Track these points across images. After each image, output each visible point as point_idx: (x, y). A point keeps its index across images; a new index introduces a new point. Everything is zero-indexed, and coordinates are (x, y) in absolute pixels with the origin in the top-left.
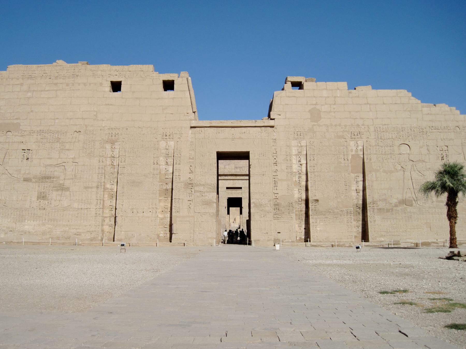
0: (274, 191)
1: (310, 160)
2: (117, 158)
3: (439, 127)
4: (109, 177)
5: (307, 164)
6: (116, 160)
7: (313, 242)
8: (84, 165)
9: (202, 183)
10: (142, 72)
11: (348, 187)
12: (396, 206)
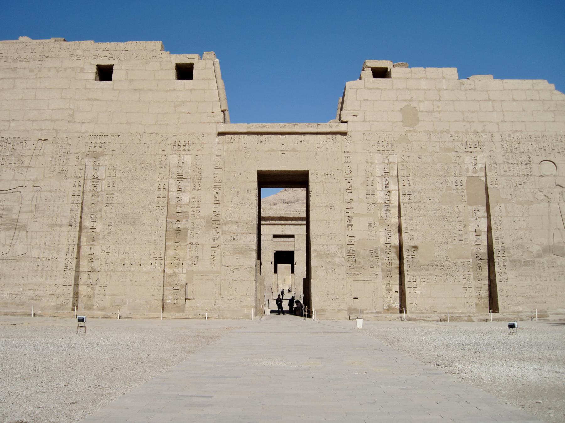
1: (404, 185)
4: (89, 209)
5: (399, 190)
6: (100, 184)
7: (411, 313)
8: (50, 191)
9: (234, 220)
10: (145, 52)
11: (463, 226)
12: (539, 256)
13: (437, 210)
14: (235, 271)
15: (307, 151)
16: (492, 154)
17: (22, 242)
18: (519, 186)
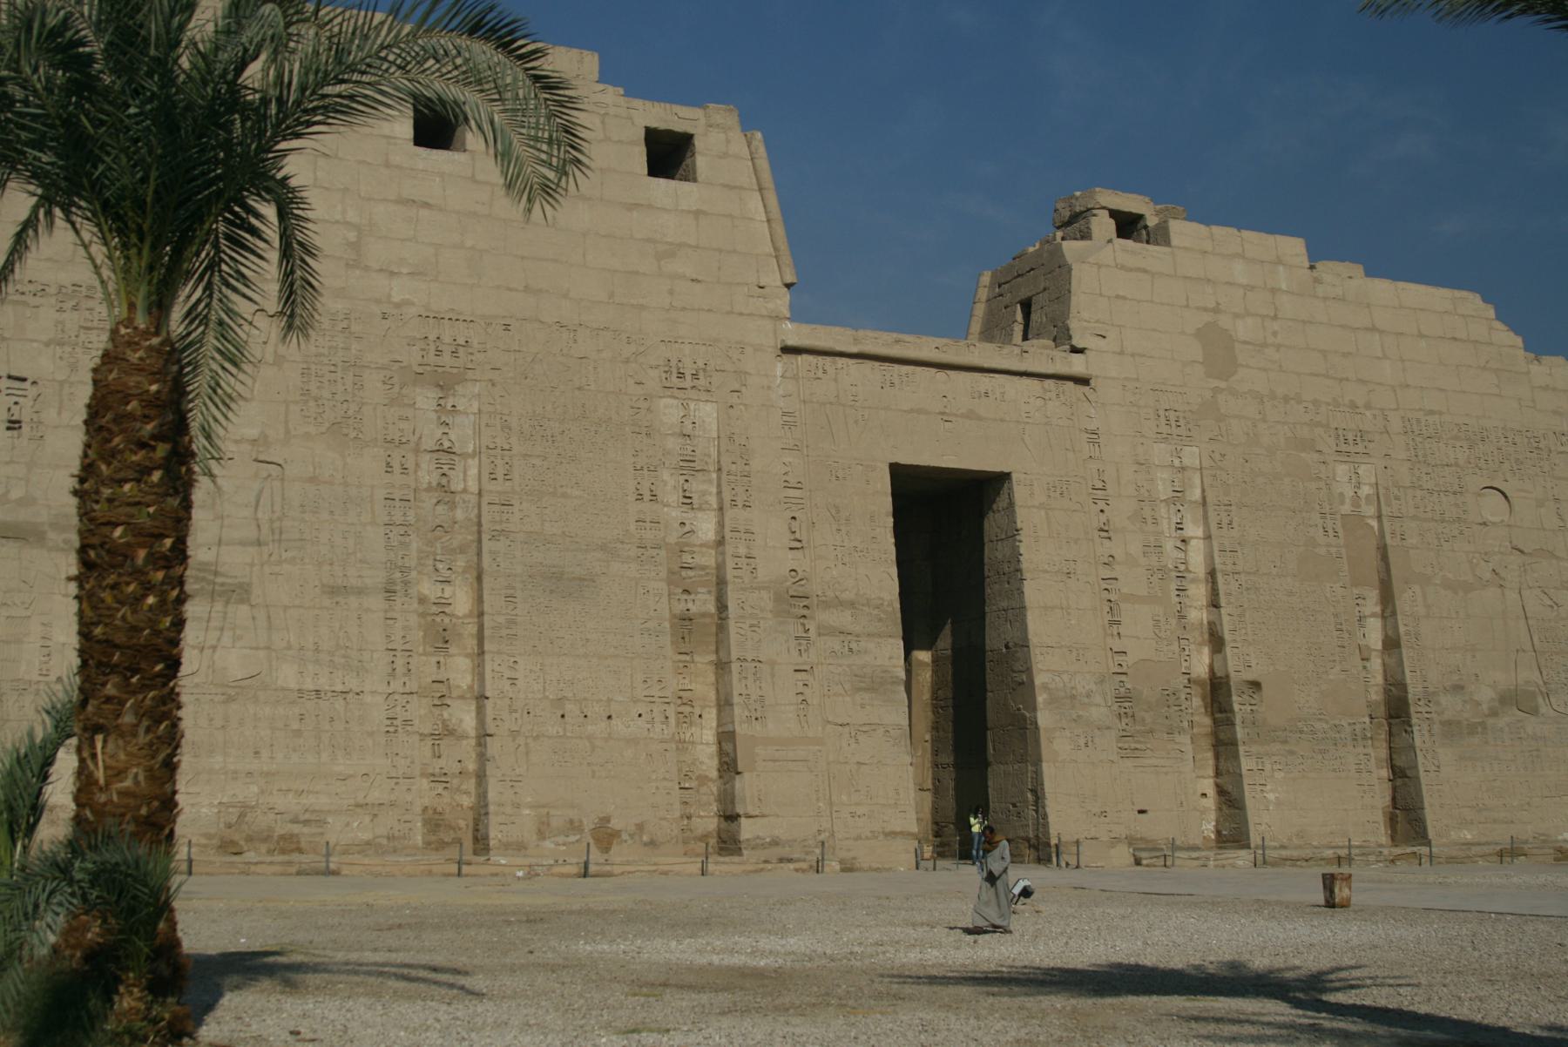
2: (464, 456)
8: (313, 480)
9: (846, 596)
11: (1346, 635)
12: (1494, 713)
13: (1291, 594)
14: (861, 738)
17: (240, 638)
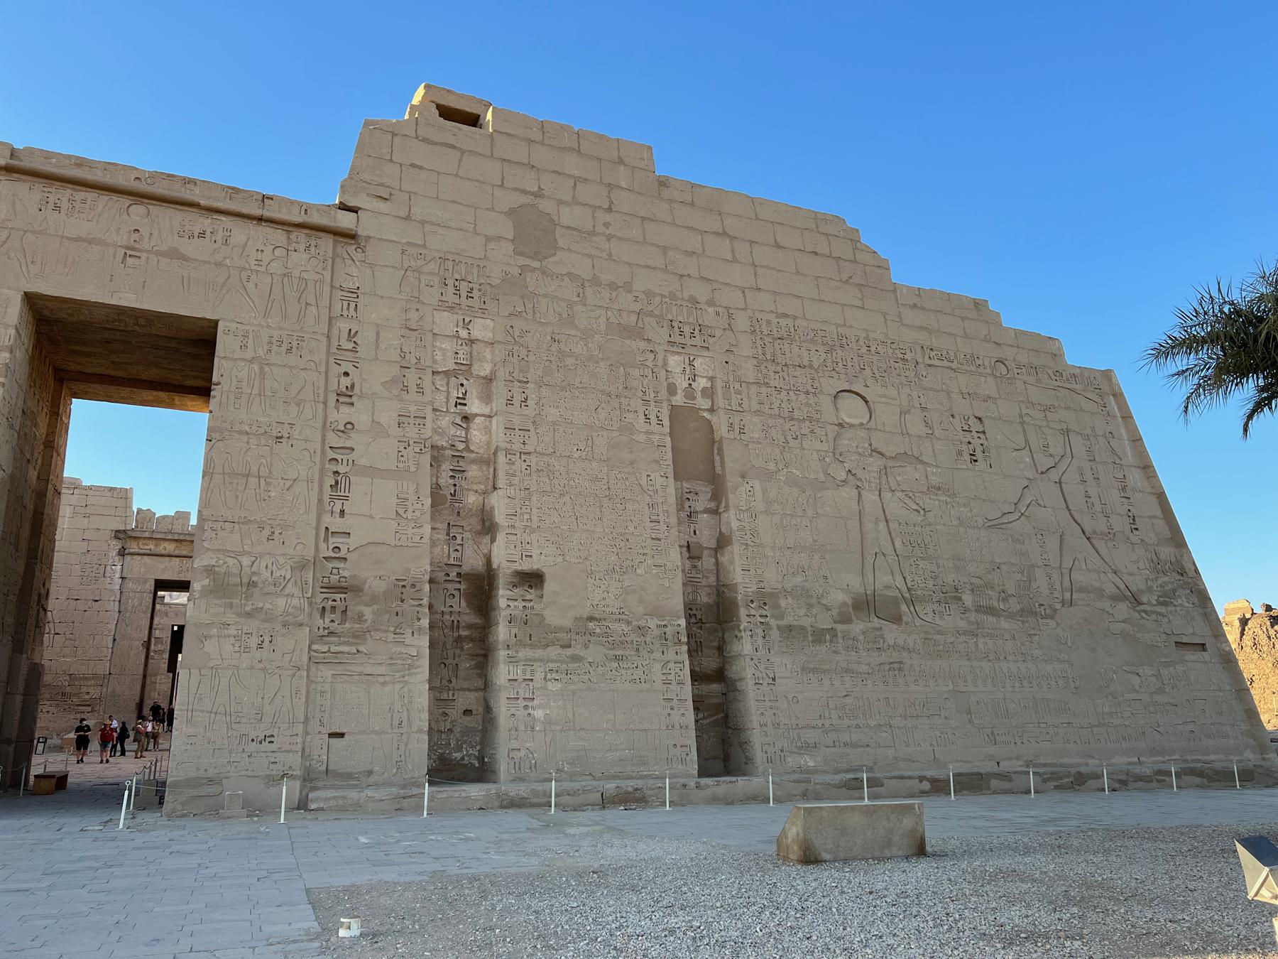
0: (327, 520)
3: (951, 353)
11: (663, 527)
13: (596, 479)
15: (219, 264)
16: (731, 358)
18: (793, 443)
